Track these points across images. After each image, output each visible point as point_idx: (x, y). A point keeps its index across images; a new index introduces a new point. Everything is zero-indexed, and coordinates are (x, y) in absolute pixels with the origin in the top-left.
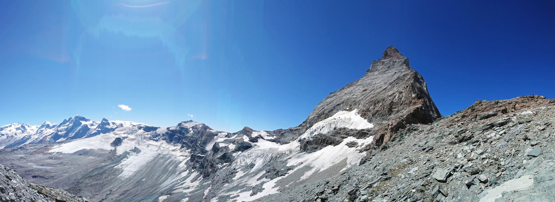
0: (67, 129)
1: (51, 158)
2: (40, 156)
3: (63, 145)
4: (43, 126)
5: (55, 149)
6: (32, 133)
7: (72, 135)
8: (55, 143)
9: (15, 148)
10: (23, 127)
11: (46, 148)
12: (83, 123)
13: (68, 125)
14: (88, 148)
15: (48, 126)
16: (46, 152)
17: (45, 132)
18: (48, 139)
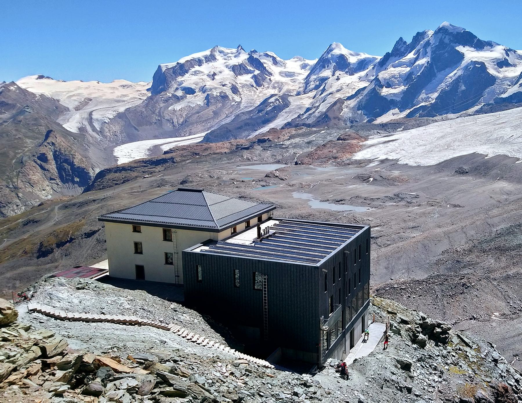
0: (407, 78)
1: (364, 179)
2: (329, 170)
3: (400, 135)
5: (374, 149)
6: (292, 86)
8: (371, 128)
9: (242, 141)
10: (252, 60)
12: (470, 55)
13: (411, 63)
14: (489, 151)
15: (342, 63)
16: (345, 157)
17: (333, 85)
18: (346, 112)
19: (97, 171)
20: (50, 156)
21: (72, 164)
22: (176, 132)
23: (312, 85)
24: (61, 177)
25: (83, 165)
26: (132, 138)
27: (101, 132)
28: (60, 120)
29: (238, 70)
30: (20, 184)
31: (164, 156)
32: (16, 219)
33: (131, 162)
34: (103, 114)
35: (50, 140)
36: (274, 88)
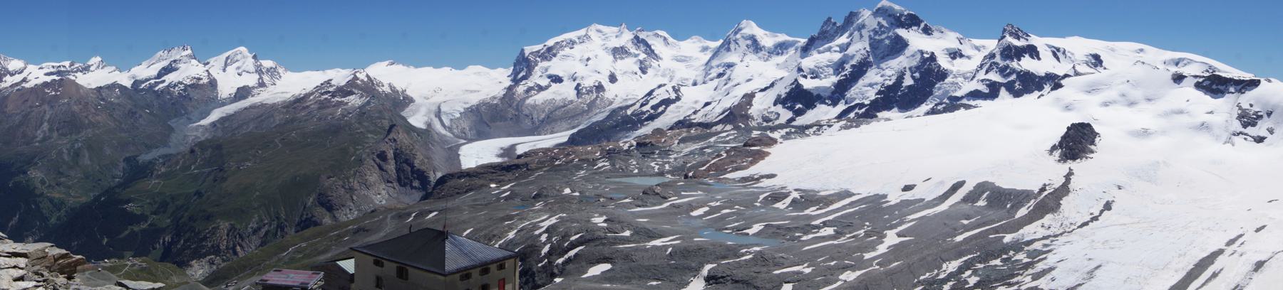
0: (839, 67)
4: (726, 46)
7: (865, 90)
11: (753, 149)
13: (843, 48)
17: (738, 73)
19: (439, 175)
20: (390, 154)
21: (412, 166)
22: (535, 130)
23: (714, 73)
24: (399, 180)
25: (423, 168)
26: (481, 135)
27: (450, 129)
28: (403, 114)
29: (619, 52)
30: (356, 185)
31: (516, 162)
32: (347, 224)
33: (478, 167)
34: (455, 108)
35: (391, 136)
36: (663, 76)
